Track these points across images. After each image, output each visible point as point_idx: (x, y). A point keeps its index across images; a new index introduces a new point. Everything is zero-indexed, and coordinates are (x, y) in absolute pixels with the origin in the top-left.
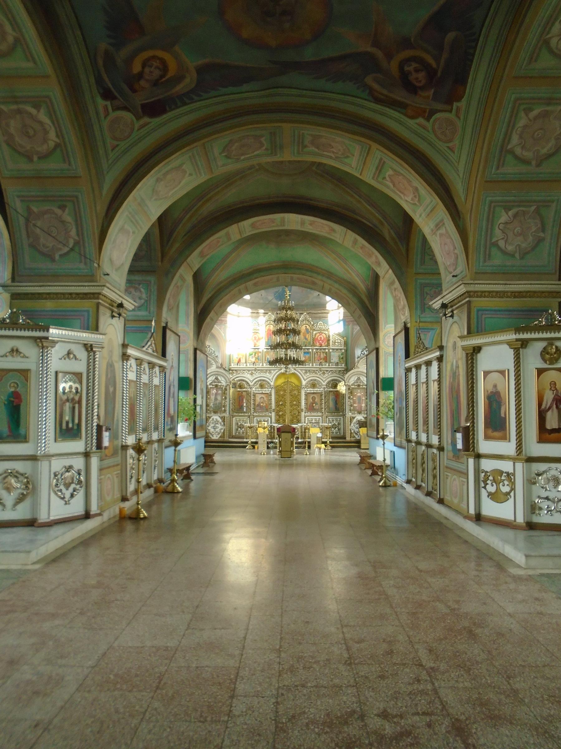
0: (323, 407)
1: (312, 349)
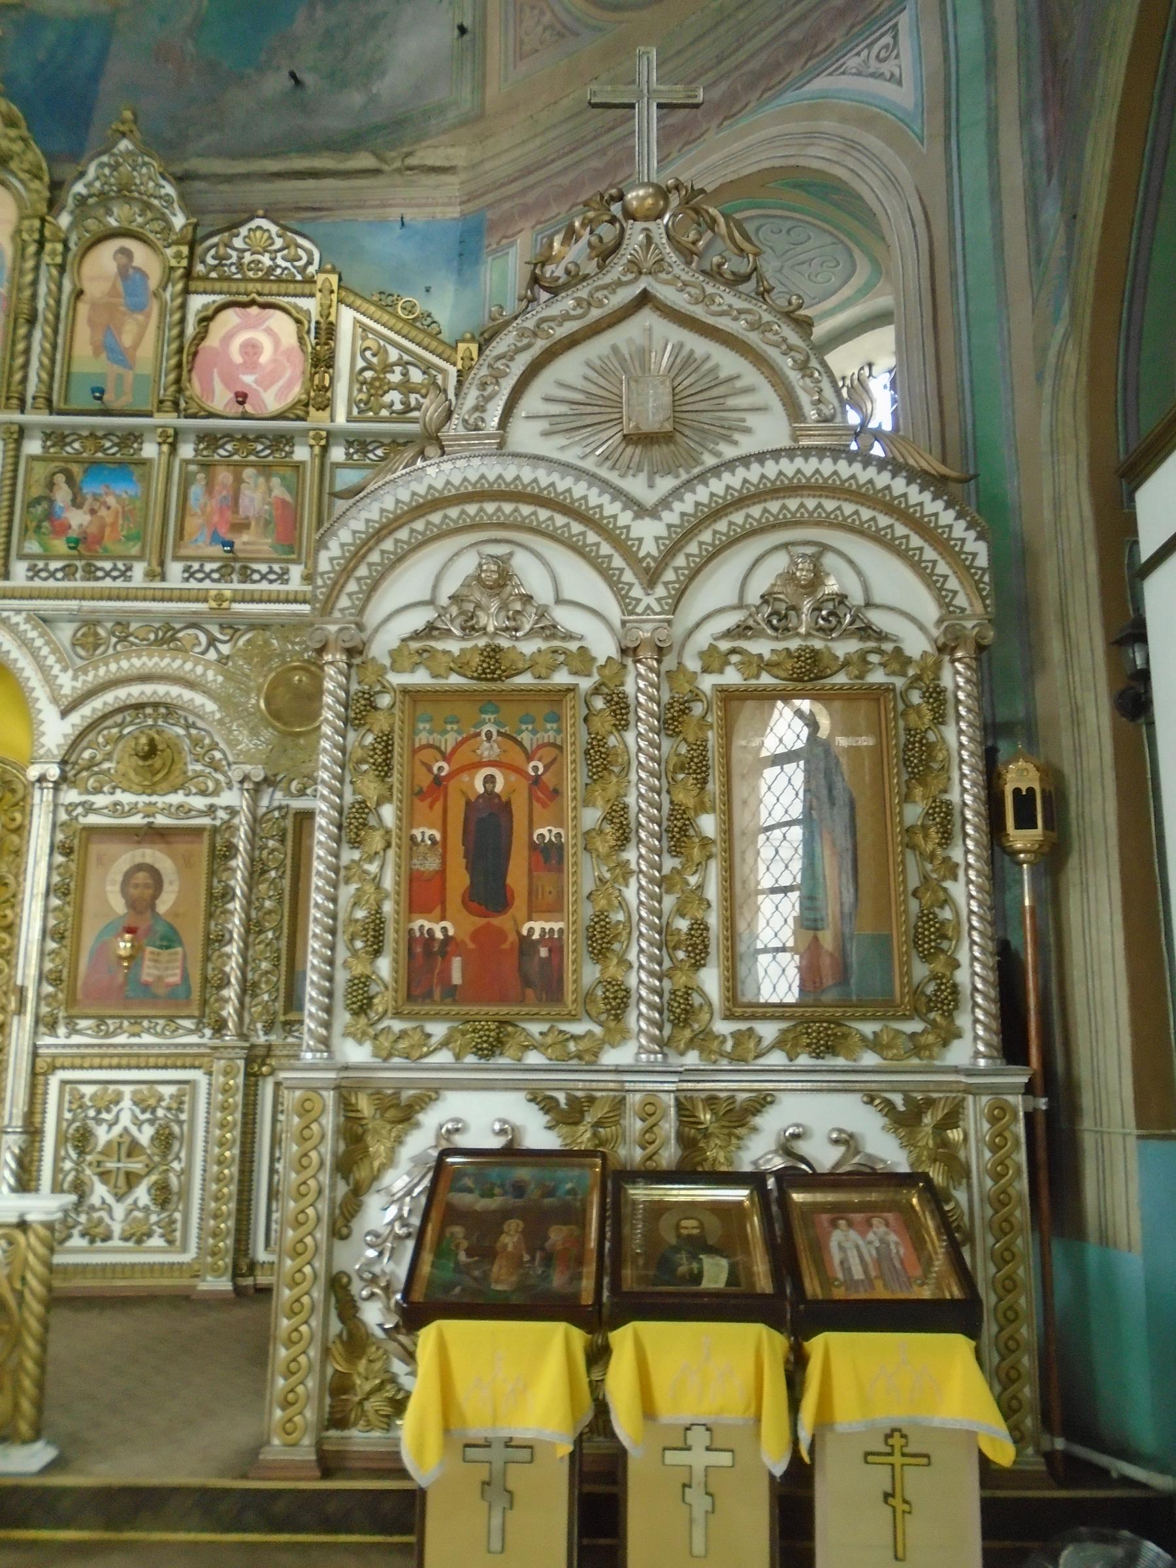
0: (232, 967)
1: (173, 441)
